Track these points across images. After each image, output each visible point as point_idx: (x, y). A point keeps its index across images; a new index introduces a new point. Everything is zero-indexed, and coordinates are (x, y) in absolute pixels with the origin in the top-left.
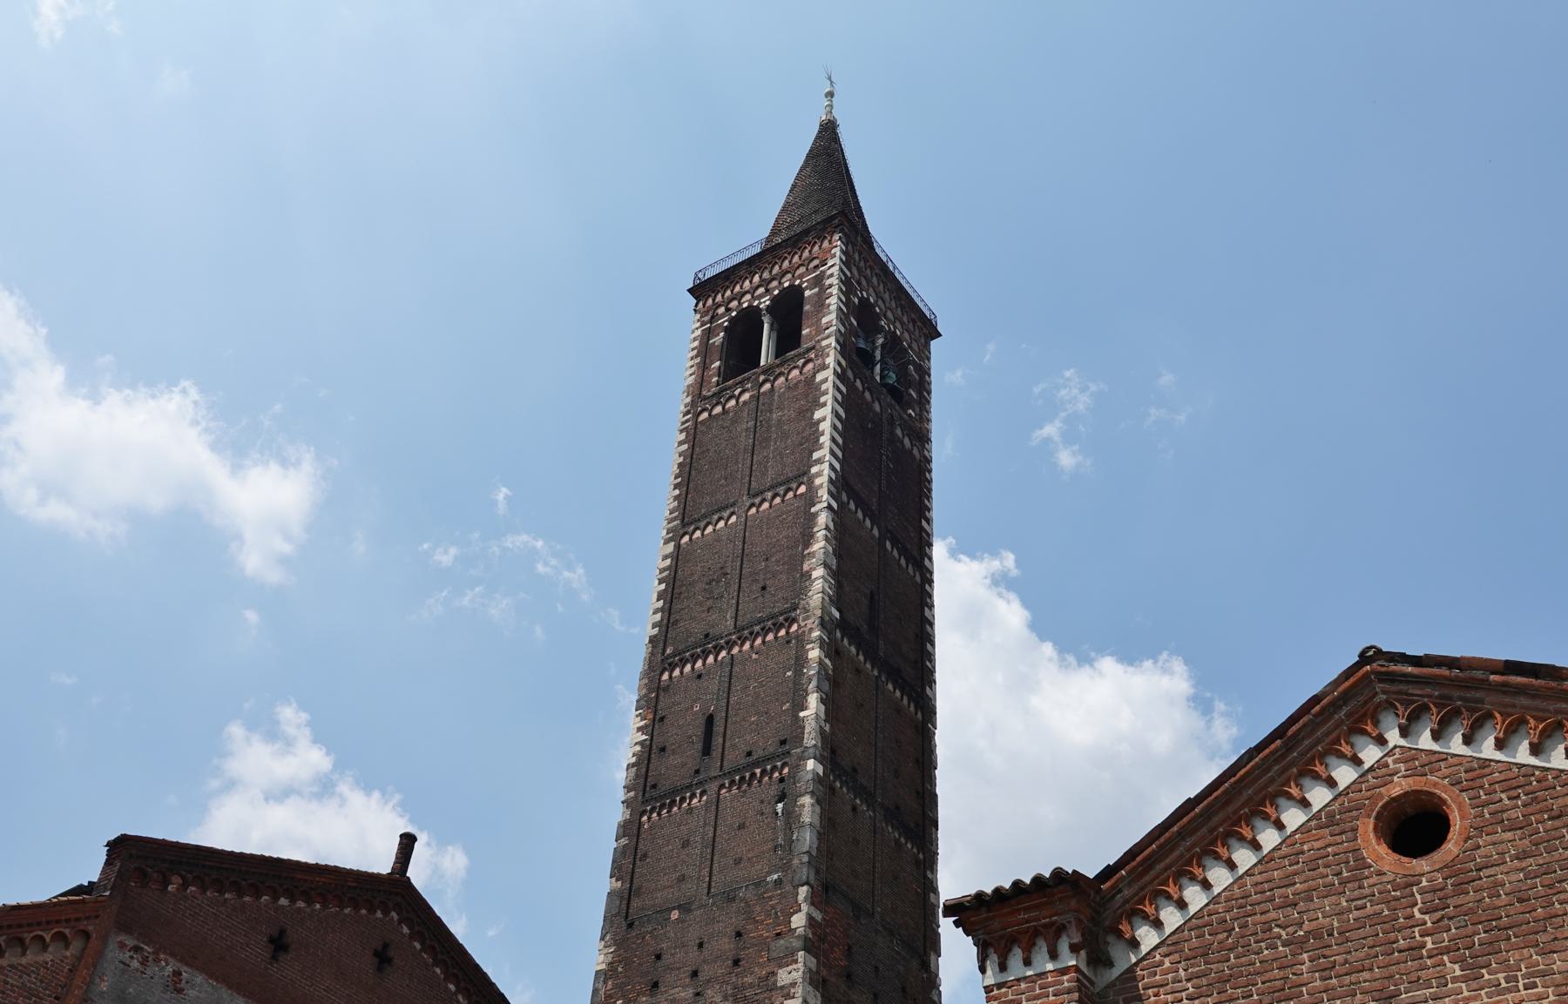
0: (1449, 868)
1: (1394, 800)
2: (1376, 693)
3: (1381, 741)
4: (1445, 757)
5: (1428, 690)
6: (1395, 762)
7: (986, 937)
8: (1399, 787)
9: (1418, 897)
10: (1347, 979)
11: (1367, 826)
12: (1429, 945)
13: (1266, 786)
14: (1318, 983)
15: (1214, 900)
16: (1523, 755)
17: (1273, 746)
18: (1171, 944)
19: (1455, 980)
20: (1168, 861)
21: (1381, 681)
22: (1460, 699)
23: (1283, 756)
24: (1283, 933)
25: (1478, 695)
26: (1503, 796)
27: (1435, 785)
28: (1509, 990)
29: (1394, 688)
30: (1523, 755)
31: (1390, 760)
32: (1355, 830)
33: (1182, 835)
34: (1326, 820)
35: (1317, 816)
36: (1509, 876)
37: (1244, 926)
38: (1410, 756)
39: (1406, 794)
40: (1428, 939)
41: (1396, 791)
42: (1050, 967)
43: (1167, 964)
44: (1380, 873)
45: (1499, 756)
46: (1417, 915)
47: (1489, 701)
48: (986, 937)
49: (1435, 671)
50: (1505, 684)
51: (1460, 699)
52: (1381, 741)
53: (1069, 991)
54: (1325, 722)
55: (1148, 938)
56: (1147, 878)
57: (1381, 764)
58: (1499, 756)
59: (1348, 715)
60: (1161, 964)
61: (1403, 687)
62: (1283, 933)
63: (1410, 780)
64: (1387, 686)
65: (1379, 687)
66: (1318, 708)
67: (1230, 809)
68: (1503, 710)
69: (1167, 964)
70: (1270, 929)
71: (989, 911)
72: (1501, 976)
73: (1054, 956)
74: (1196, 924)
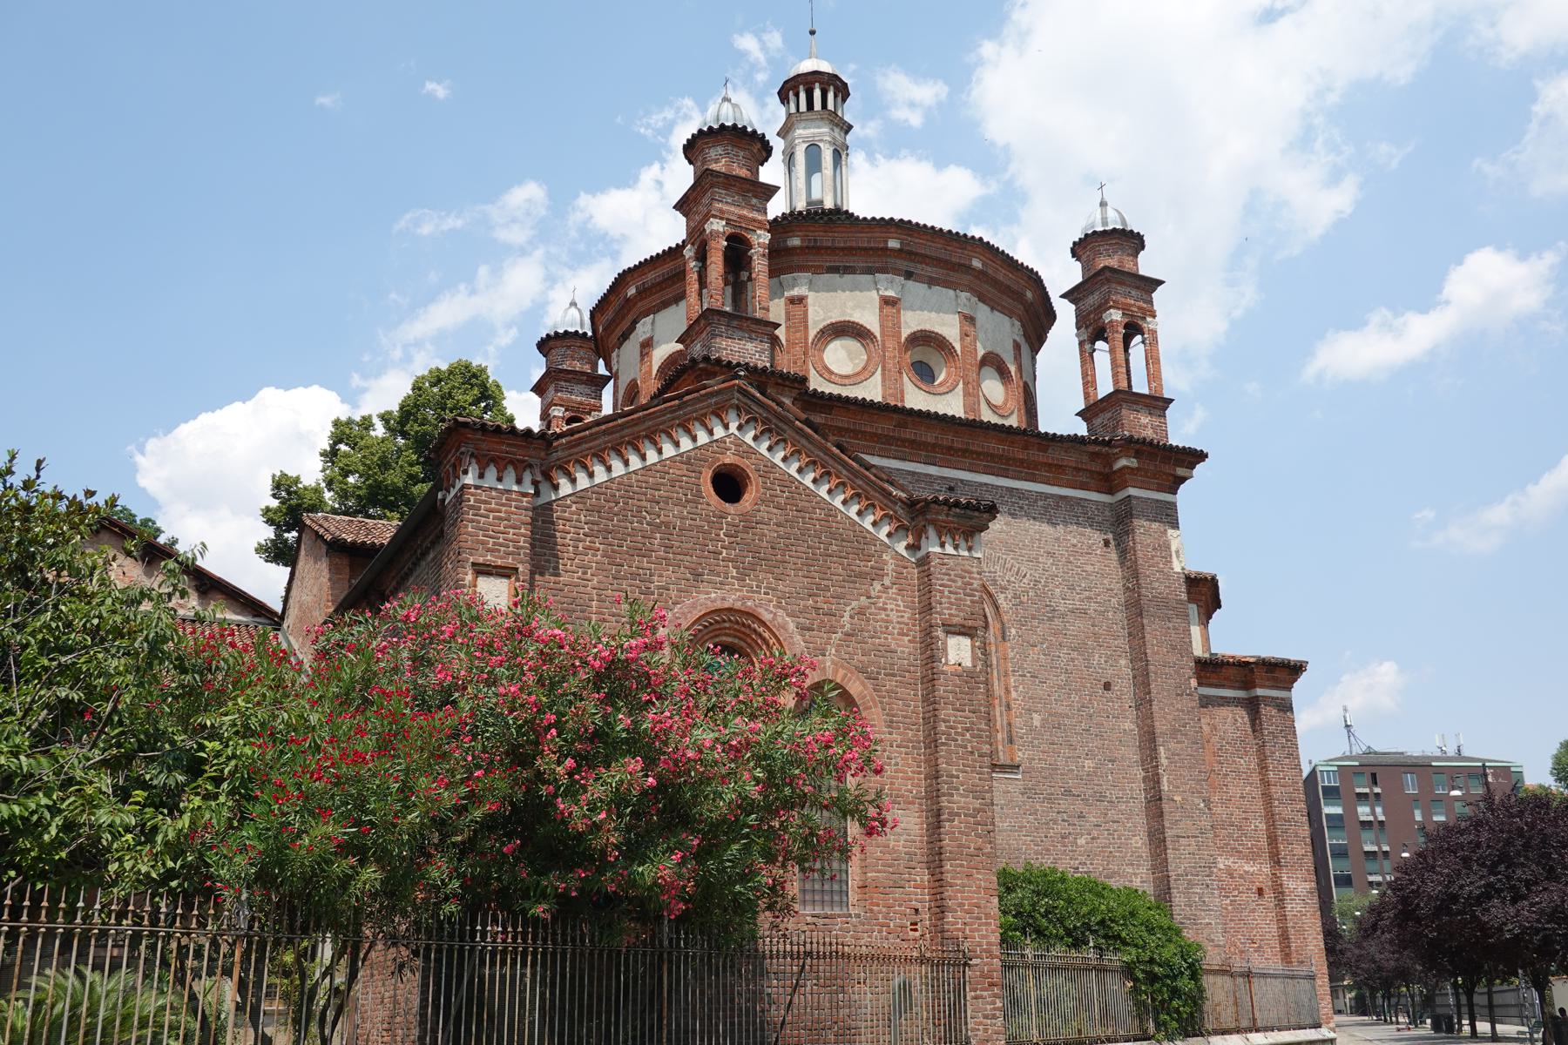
0: (744, 516)
1: (725, 465)
3: (726, 427)
4: (755, 452)
5: (761, 411)
6: (730, 442)
7: (476, 452)
8: (729, 458)
10: (679, 557)
11: (707, 475)
12: (724, 554)
13: (659, 425)
14: (662, 553)
15: (611, 480)
16: (792, 470)
17: (673, 403)
18: (580, 497)
19: (733, 577)
20: (591, 444)
21: (738, 392)
22: (776, 425)
23: (675, 411)
24: (648, 517)
25: (785, 427)
27: (748, 466)
28: (757, 592)
29: (745, 400)
30: (792, 470)
31: (728, 440)
33: (605, 432)
34: (686, 460)
35: (681, 455)
36: (770, 532)
38: (739, 443)
39: (731, 464)
40: (724, 551)
41: (727, 461)
42: (515, 488)
43: (574, 508)
44: (708, 504)
45: (781, 465)
46: (722, 536)
47: (789, 433)
48: (476, 452)
49: (770, 402)
50: (801, 429)
51: (776, 425)
52: (726, 427)
53: (526, 509)
54: (702, 401)
55: (565, 488)
56: (575, 450)
57: (721, 441)
58: (781, 465)
59: (716, 403)
60: (570, 507)
61: (749, 402)
62: (648, 517)
63: (737, 457)
65: (737, 395)
67: (636, 429)
69: (574, 508)
71: (483, 435)
72: (755, 583)
73: (519, 481)
74: (597, 490)
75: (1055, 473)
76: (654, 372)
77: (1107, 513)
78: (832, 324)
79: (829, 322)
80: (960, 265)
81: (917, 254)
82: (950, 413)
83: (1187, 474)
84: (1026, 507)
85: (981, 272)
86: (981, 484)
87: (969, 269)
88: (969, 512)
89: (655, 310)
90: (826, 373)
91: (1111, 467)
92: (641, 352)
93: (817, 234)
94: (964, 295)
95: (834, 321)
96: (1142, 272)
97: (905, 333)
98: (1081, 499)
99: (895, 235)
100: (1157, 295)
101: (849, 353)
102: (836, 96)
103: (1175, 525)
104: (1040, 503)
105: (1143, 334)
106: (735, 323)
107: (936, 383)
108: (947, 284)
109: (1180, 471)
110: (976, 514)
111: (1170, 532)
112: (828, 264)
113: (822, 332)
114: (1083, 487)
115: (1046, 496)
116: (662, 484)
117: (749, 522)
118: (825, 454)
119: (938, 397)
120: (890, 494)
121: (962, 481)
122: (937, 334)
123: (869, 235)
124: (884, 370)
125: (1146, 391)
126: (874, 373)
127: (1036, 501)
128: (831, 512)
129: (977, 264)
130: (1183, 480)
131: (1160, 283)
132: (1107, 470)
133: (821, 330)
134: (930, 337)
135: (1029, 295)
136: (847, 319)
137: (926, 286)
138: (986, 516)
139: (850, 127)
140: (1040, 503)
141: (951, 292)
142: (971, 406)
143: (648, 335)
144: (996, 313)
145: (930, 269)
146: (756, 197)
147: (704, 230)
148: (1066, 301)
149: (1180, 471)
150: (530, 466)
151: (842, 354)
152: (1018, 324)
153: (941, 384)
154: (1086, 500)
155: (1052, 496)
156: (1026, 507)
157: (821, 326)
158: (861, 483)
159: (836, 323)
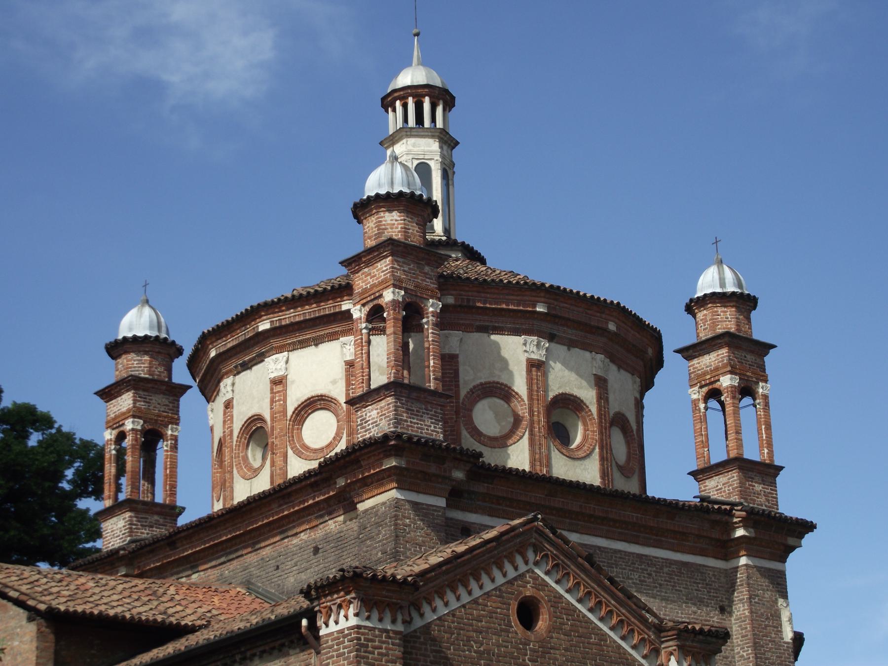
0: (542, 642)
1: (526, 597)
2: (532, 537)
8: (529, 592)
9: (528, 652)
21: (536, 532)
26: (564, 616)
27: (542, 598)
32: (509, 604)
37: (459, 634)
41: (528, 594)
46: (527, 661)
64: (537, 536)
65: (535, 535)
66: (513, 534)
68: (574, 574)
69: (422, 640)
70: (470, 641)
75: (679, 542)
76: (290, 412)
77: (723, 580)
78: (481, 384)
79: (478, 382)
80: (598, 328)
81: (560, 317)
82: (588, 482)
83: (796, 544)
84: (654, 574)
85: (615, 334)
86: (616, 551)
87: (606, 330)
88: (709, 638)
89: (293, 347)
90: (476, 433)
91: (729, 534)
92: (272, 389)
93: (470, 293)
94: (600, 357)
95: (483, 381)
96: (756, 336)
97: (551, 395)
98: (700, 565)
99: (543, 299)
100: (770, 360)
101: (496, 414)
102: (444, 110)
103: (785, 596)
104: (666, 570)
105: (754, 399)
106: (414, 395)
107: (574, 446)
108: (586, 347)
109: (791, 541)
110: (714, 640)
111: (781, 601)
112: (478, 323)
113: (472, 391)
114: (703, 553)
115: (669, 562)
116: (483, 616)
117: (545, 648)
118: (599, 586)
119: (577, 463)
120: (646, 620)
121: (599, 548)
122: (576, 397)
123: (519, 298)
124: (532, 434)
125: (756, 458)
126: (521, 437)
127: (661, 569)
128: (603, 636)
129: (612, 327)
130: (792, 549)
131: (773, 346)
132: (725, 537)
133: (471, 390)
134: (569, 399)
135: (650, 351)
136: (496, 379)
137: (565, 348)
138: (720, 641)
139: (457, 143)
140: (666, 570)
141: (587, 354)
142: (604, 474)
143: (281, 373)
144: (622, 371)
145: (570, 331)
146: (428, 264)
147: (381, 296)
148: (679, 355)
149: (791, 541)
150: (401, 608)
151: (489, 415)
152: (638, 380)
153: (579, 448)
154: (704, 566)
155: (676, 562)
156: (654, 574)
157: (471, 386)
158: (624, 611)
159: (486, 383)
